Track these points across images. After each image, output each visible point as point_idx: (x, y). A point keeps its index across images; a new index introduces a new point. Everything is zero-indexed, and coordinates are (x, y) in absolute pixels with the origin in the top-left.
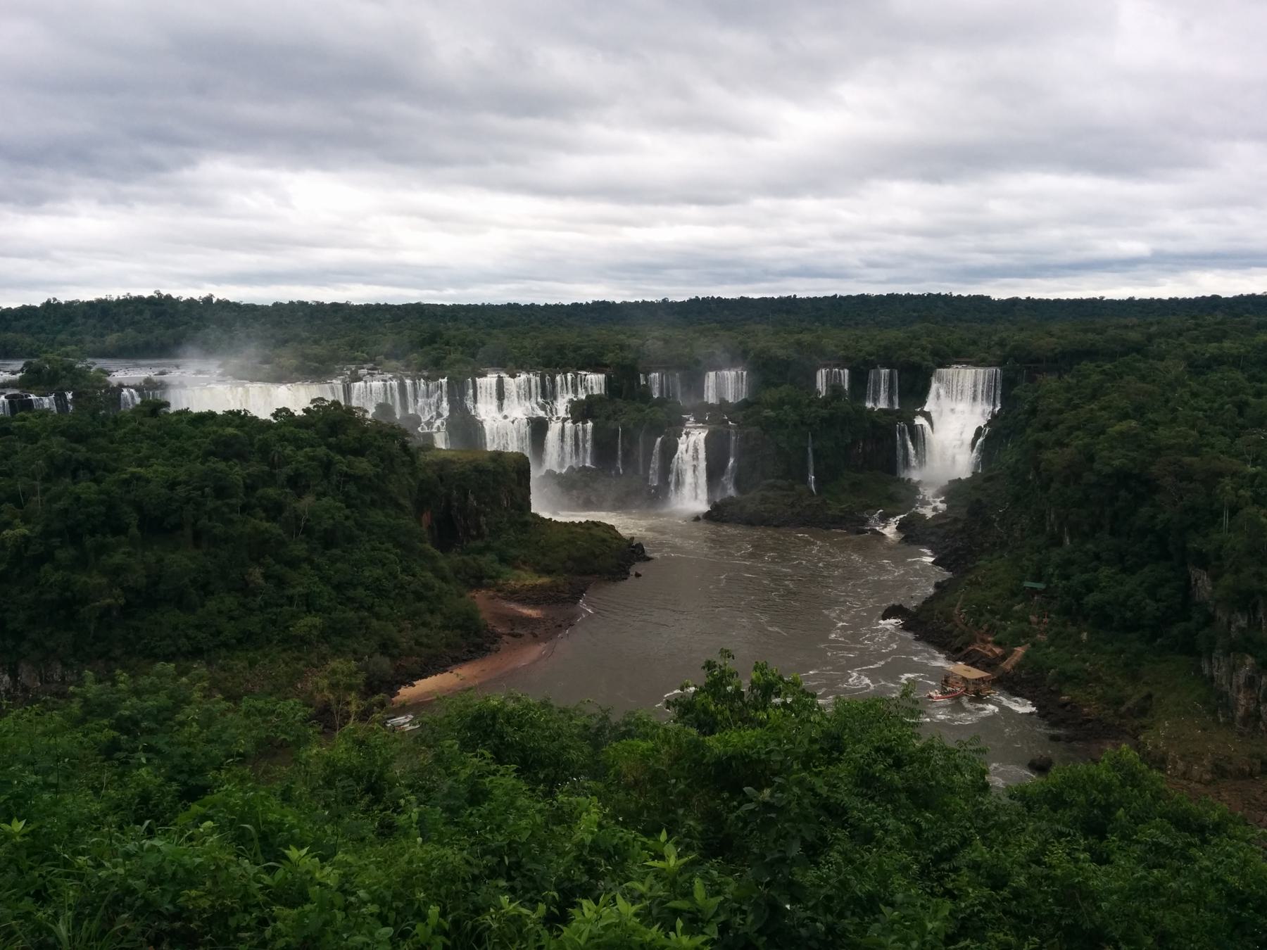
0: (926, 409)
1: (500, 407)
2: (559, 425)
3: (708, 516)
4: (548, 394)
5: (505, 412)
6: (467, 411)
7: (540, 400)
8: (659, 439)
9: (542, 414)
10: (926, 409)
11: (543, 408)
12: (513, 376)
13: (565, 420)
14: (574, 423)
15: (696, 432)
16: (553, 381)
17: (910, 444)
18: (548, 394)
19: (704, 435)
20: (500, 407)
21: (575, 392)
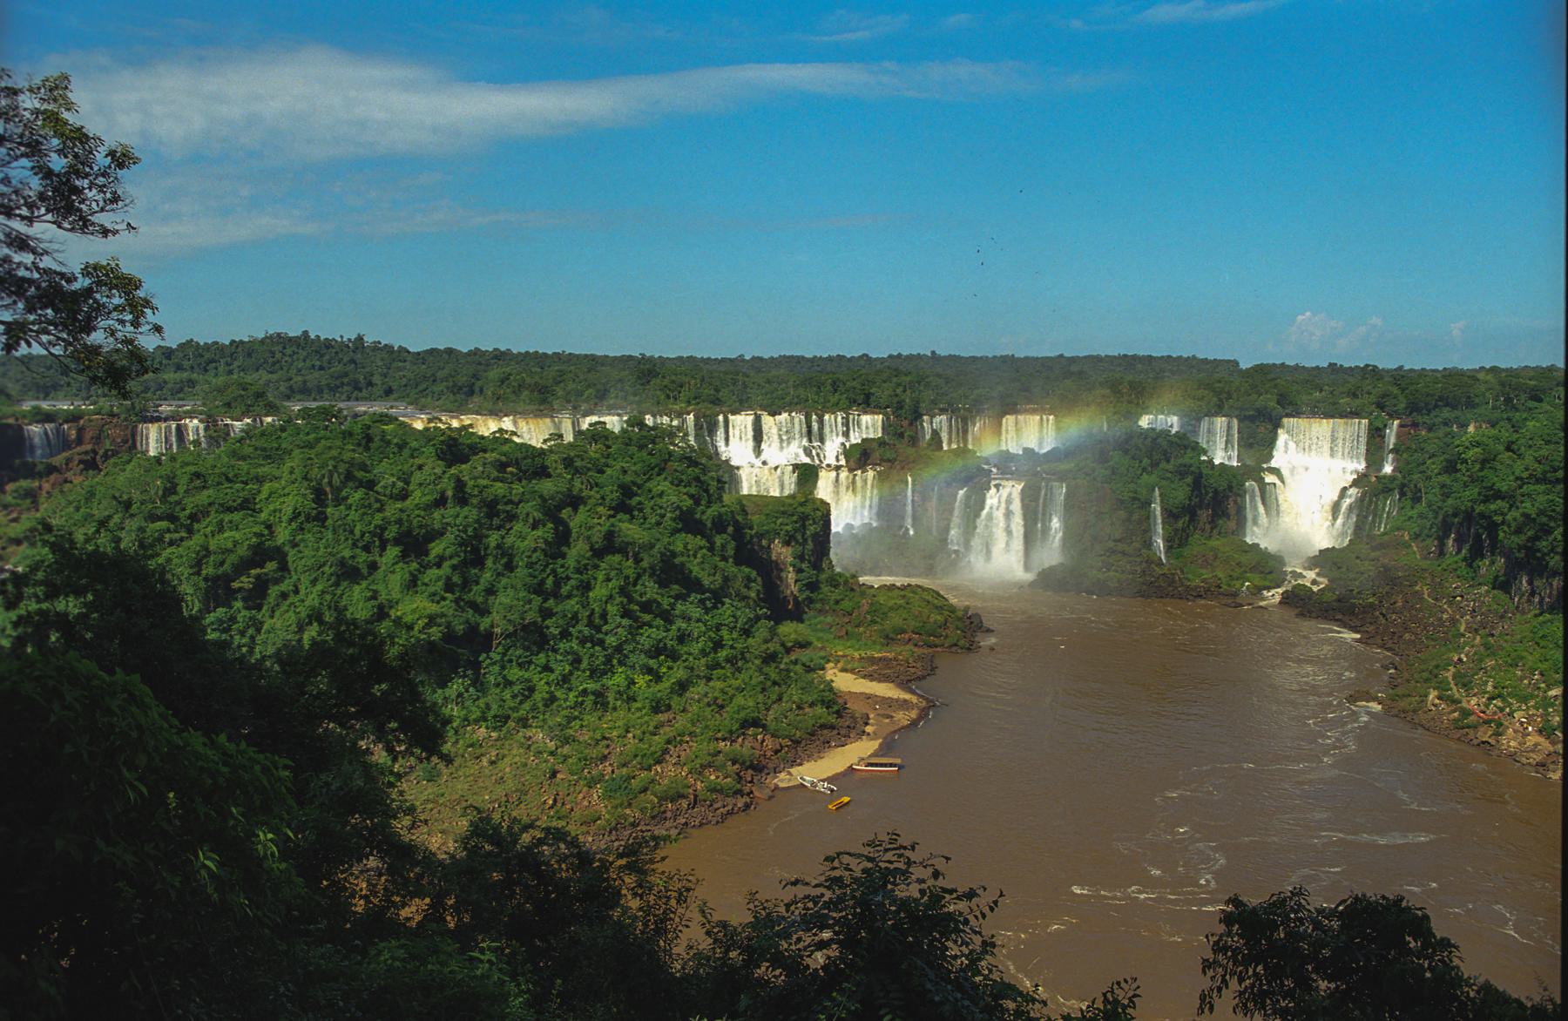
0: (1273, 464)
1: (758, 450)
2: (834, 474)
3: (1032, 584)
4: (814, 435)
5: (763, 457)
6: (717, 454)
7: (805, 442)
8: (961, 492)
9: (807, 460)
10: (1273, 464)
11: (807, 452)
12: (773, 414)
13: (838, 468)
14: (851, 470)
15: (1011, 483)
16: (821, 422)
17: (1261, 509)
18: (814, 435)
19: (1019, 487)
20: (758, 450)
21: (846, 434)
